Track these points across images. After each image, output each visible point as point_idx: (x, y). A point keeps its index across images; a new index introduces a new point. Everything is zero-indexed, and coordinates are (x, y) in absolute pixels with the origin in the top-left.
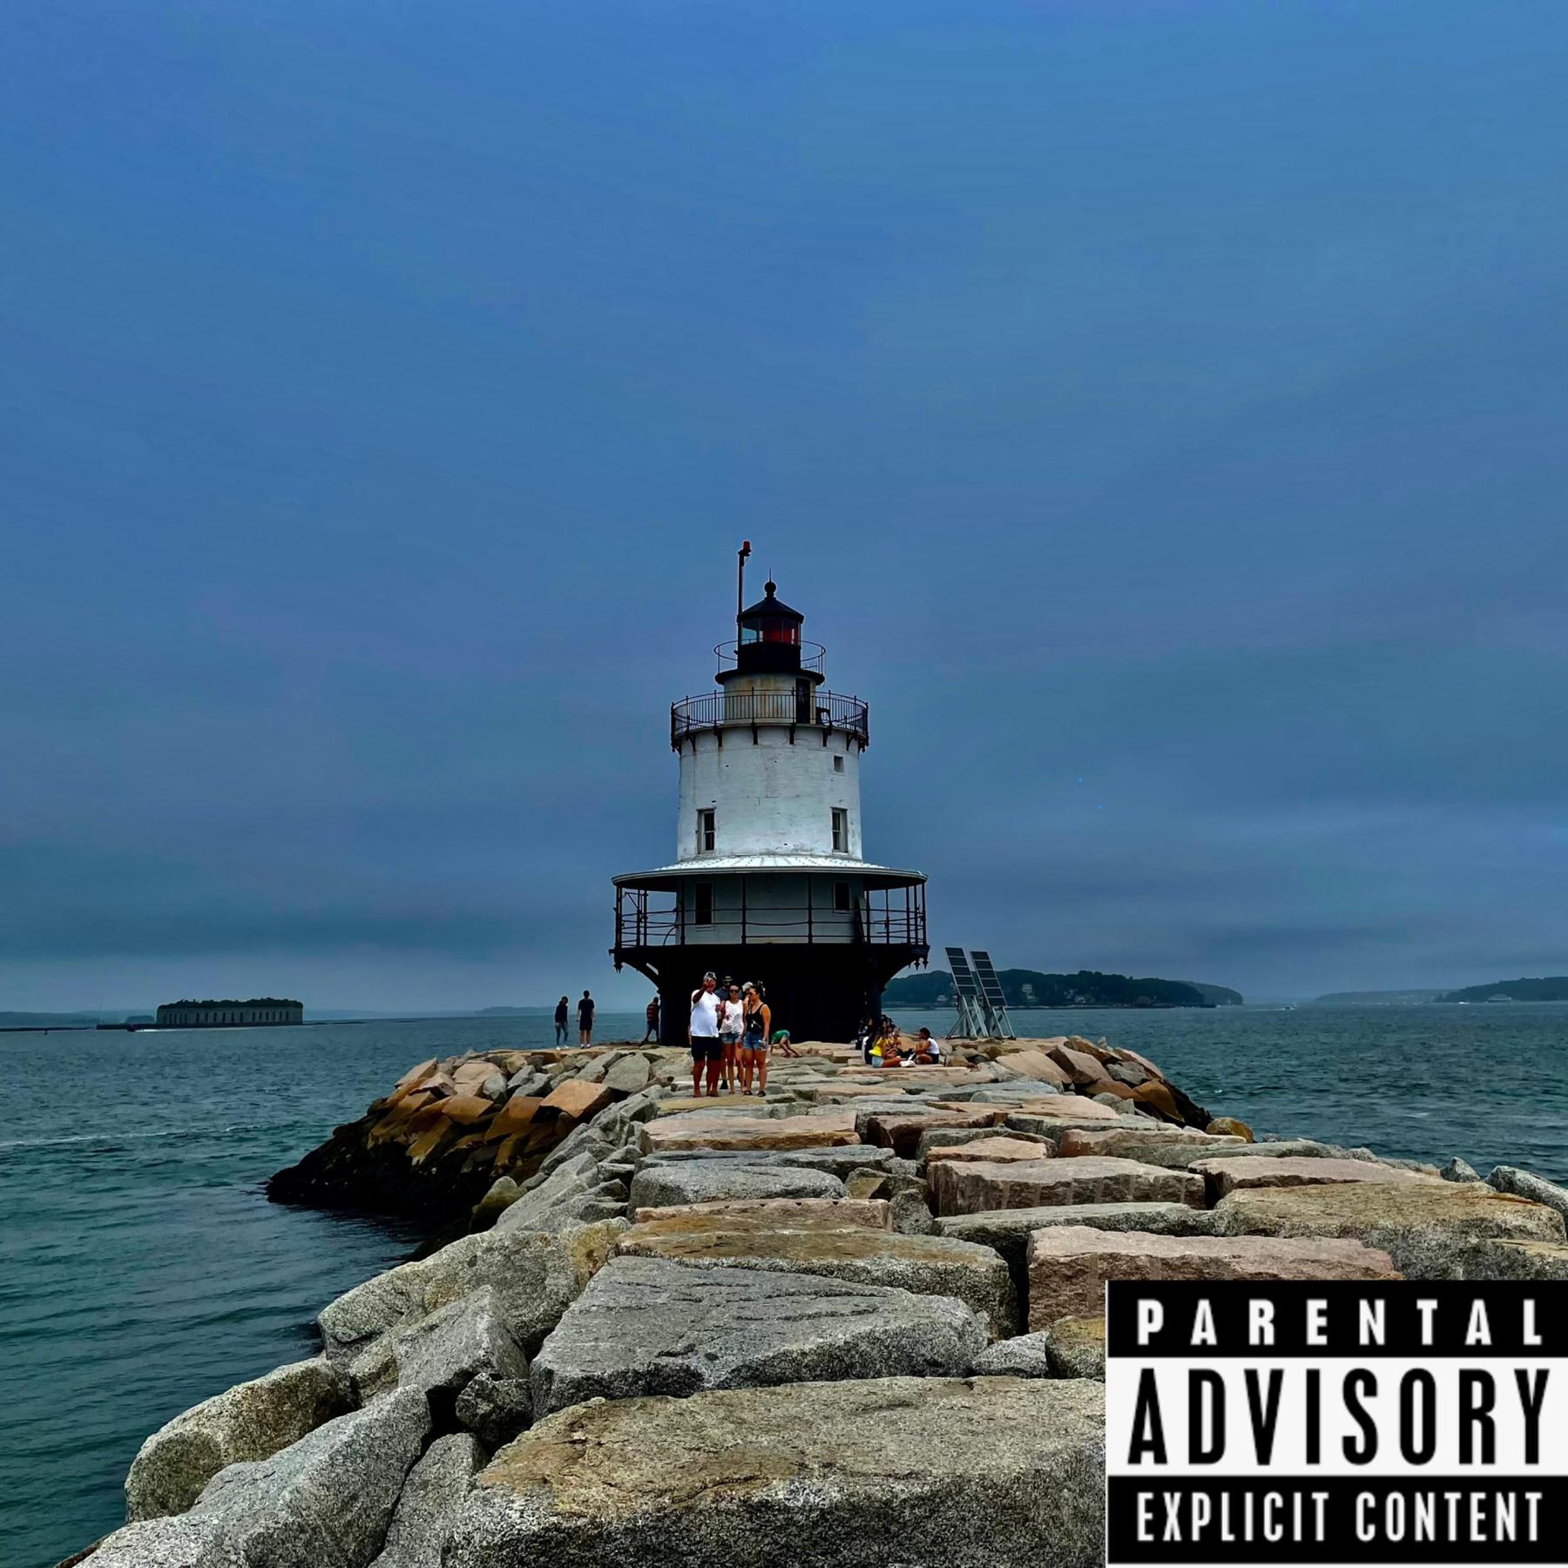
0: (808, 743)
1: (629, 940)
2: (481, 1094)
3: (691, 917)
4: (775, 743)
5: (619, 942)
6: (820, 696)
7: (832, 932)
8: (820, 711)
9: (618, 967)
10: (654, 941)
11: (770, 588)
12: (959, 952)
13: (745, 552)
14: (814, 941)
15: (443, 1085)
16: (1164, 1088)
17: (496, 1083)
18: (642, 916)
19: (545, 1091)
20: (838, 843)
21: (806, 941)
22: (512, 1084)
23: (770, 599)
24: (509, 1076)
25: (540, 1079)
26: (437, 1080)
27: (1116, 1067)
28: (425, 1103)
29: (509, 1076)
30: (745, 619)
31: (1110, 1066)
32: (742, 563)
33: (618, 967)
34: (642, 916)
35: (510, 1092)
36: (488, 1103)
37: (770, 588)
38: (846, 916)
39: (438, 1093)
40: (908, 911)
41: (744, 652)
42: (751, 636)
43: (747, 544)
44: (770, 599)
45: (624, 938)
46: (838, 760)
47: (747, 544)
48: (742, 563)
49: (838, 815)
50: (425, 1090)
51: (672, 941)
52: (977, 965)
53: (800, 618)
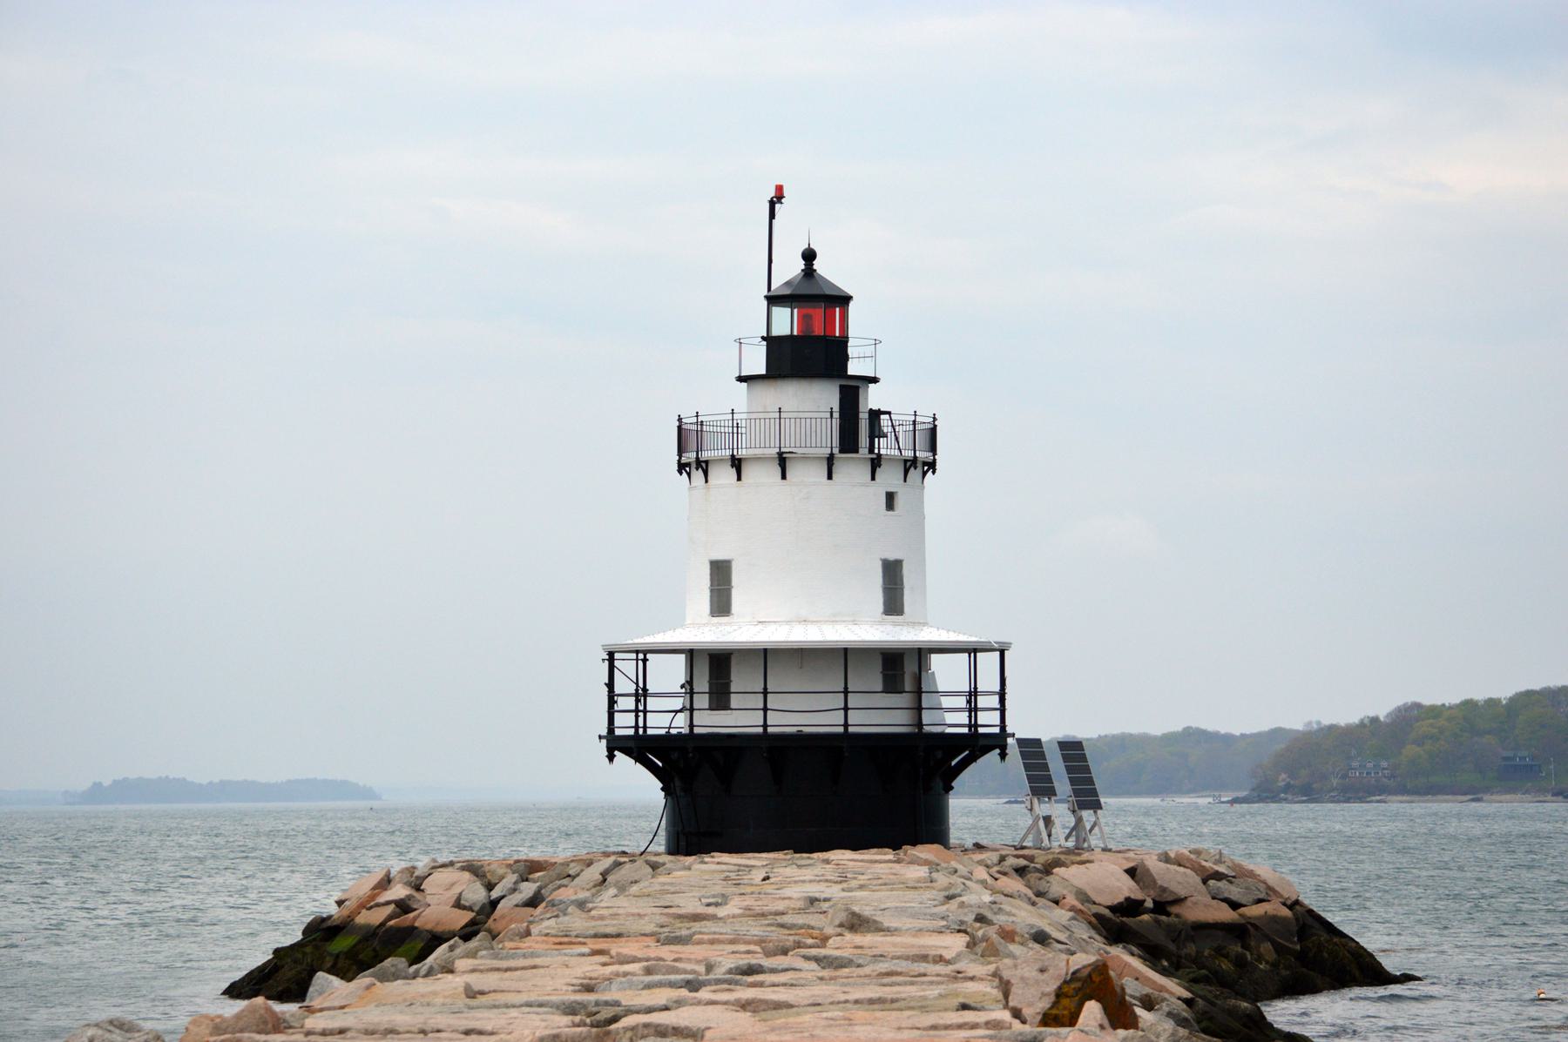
0: (852, 471)
1: (625, 724)
2: (458, 904)
3: (702, 701)
5: (611, 729)
6: (873, 398)
7: (878, 715)
8: (875, 415)
9: (611, 757)
10: (657, 724)
11: (809, 256)
12: (1037, 742)
13: (779, 196)
14: (851, 729)
15: (409, 897)
16: (1286, 912)
18: (642, 694)
20: (893, 604)
21: (841, 730)
22: (495, 894)
23: (809, 272)
24: (490, 887)
25: (528, 889)
26: (399, 891)
27: (1222, 884)
28: (390, 918)
29: (490, 887)
30: (773, 300)
31: (1211, 882)
32: (772, 215)
33: (611, 757)
34: (642, 694)
35: (494, 904)
36: (469, 916)
37: (809, 256)
39: (403, 907)
40: (973, 694)
41: (772, 342)
42: (784, 322)
43: (779, 189)
44: (809, 272)
45: (620, 719)
46: (890, 499)
47: (779, 189)
48: (772, 215)
50: (388, 903)
51: (680, 724)
52: (1065, 758)
53: (844, 300)
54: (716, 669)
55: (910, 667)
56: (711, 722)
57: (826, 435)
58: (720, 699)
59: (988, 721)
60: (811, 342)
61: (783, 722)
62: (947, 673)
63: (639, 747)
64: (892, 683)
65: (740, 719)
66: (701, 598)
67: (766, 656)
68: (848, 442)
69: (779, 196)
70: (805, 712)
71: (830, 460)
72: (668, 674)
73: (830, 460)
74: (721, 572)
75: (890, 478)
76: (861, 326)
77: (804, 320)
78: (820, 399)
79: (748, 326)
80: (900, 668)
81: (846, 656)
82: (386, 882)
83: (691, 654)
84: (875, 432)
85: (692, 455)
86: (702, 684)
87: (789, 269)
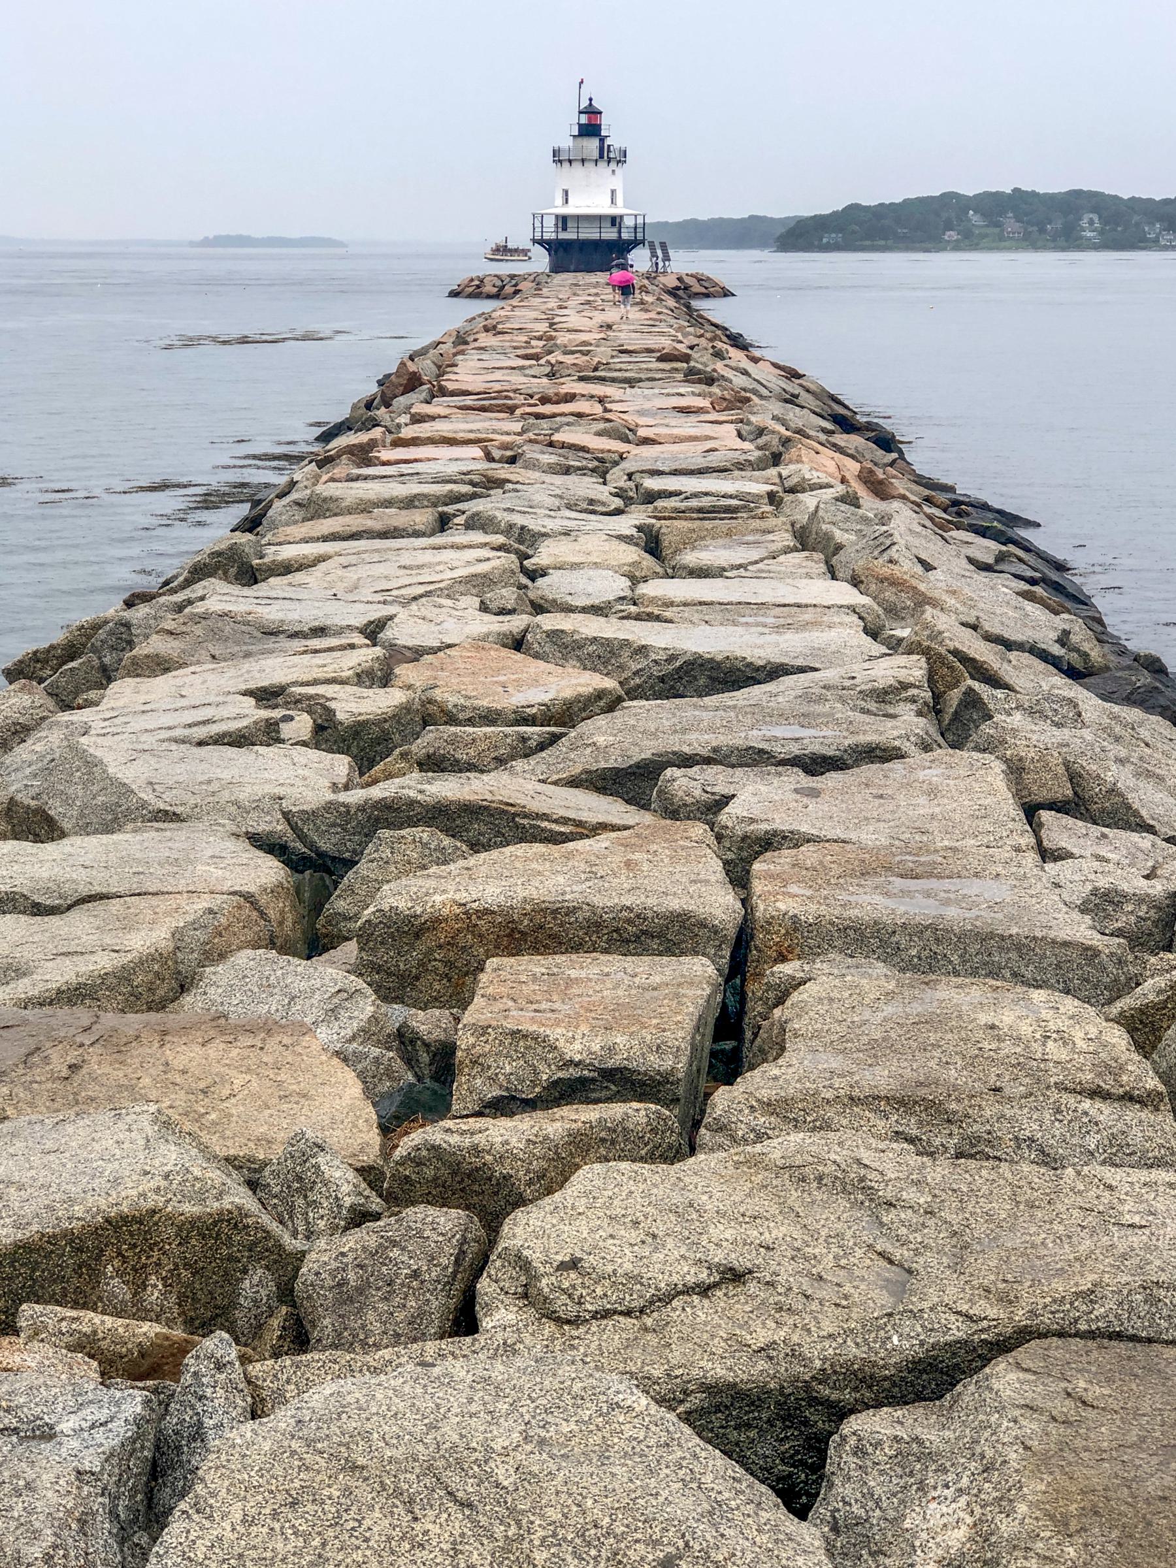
0: (602, 164)
1: (538, 236)
4: (590, 166)
6: (608, 142)
7: (610, 234)
10: (546, 236)
11: (591, 100)
13: (582, 82)
17: (499, 283)
19: (515, 286)
23: (590, 104)
26: (477, 283)
30: (580, 112)
37: (591, 100)
38: (615, 230)
39: (478, 287)
40: (636, 228)
42: (584, 119)
44: (590, 104)
49: (613, 192)
51: (553, 236)
54: (563, 221)
55: (618, 220)
56: (563, 236)
57: (596, 155)
58: (565, 229)
59: (640, 236)
60: (590, 127)
61: (582, 236)
62: (629, 222)
63: (541, 242)
64: (613, 223)
65: (570, 235)
66: (559, 200)
67: (578, 218)
68: (601, 157)
69: (582, 82)
70: (589, 233)
71: (596, 161)
72: (550, 223)
73: (596, 161)
74: (566, 192)
75: (613, 165)
76: (605, 121)
77: (589, 118)
78: (594, 143)
79: (572, 120)
80: (615, 221)
81: (600, 218)
82: (472, 280)
83: (557, 216)
84: (609, 151)
85: (558, 157)
86: (560, 225)
87: (585, 104)
